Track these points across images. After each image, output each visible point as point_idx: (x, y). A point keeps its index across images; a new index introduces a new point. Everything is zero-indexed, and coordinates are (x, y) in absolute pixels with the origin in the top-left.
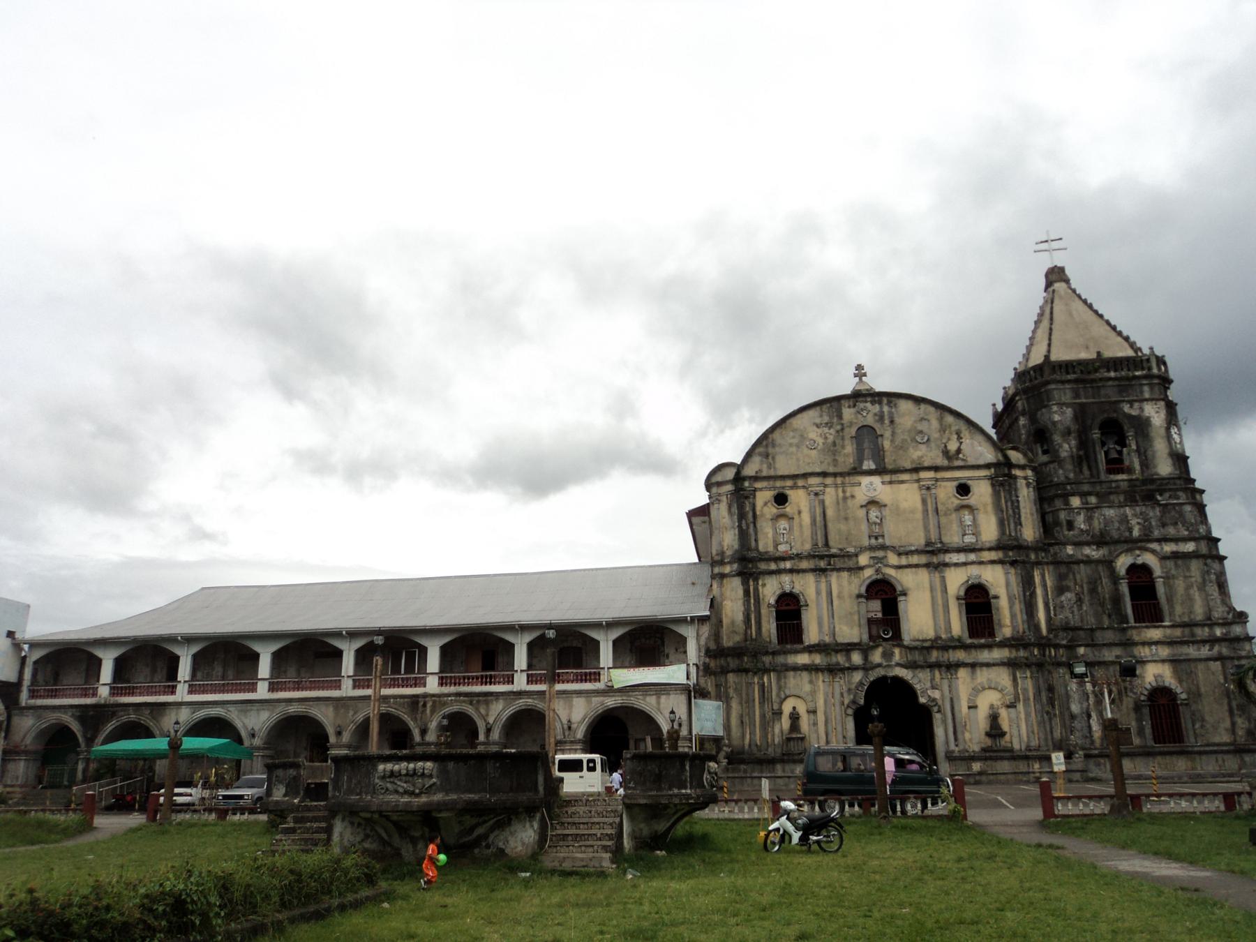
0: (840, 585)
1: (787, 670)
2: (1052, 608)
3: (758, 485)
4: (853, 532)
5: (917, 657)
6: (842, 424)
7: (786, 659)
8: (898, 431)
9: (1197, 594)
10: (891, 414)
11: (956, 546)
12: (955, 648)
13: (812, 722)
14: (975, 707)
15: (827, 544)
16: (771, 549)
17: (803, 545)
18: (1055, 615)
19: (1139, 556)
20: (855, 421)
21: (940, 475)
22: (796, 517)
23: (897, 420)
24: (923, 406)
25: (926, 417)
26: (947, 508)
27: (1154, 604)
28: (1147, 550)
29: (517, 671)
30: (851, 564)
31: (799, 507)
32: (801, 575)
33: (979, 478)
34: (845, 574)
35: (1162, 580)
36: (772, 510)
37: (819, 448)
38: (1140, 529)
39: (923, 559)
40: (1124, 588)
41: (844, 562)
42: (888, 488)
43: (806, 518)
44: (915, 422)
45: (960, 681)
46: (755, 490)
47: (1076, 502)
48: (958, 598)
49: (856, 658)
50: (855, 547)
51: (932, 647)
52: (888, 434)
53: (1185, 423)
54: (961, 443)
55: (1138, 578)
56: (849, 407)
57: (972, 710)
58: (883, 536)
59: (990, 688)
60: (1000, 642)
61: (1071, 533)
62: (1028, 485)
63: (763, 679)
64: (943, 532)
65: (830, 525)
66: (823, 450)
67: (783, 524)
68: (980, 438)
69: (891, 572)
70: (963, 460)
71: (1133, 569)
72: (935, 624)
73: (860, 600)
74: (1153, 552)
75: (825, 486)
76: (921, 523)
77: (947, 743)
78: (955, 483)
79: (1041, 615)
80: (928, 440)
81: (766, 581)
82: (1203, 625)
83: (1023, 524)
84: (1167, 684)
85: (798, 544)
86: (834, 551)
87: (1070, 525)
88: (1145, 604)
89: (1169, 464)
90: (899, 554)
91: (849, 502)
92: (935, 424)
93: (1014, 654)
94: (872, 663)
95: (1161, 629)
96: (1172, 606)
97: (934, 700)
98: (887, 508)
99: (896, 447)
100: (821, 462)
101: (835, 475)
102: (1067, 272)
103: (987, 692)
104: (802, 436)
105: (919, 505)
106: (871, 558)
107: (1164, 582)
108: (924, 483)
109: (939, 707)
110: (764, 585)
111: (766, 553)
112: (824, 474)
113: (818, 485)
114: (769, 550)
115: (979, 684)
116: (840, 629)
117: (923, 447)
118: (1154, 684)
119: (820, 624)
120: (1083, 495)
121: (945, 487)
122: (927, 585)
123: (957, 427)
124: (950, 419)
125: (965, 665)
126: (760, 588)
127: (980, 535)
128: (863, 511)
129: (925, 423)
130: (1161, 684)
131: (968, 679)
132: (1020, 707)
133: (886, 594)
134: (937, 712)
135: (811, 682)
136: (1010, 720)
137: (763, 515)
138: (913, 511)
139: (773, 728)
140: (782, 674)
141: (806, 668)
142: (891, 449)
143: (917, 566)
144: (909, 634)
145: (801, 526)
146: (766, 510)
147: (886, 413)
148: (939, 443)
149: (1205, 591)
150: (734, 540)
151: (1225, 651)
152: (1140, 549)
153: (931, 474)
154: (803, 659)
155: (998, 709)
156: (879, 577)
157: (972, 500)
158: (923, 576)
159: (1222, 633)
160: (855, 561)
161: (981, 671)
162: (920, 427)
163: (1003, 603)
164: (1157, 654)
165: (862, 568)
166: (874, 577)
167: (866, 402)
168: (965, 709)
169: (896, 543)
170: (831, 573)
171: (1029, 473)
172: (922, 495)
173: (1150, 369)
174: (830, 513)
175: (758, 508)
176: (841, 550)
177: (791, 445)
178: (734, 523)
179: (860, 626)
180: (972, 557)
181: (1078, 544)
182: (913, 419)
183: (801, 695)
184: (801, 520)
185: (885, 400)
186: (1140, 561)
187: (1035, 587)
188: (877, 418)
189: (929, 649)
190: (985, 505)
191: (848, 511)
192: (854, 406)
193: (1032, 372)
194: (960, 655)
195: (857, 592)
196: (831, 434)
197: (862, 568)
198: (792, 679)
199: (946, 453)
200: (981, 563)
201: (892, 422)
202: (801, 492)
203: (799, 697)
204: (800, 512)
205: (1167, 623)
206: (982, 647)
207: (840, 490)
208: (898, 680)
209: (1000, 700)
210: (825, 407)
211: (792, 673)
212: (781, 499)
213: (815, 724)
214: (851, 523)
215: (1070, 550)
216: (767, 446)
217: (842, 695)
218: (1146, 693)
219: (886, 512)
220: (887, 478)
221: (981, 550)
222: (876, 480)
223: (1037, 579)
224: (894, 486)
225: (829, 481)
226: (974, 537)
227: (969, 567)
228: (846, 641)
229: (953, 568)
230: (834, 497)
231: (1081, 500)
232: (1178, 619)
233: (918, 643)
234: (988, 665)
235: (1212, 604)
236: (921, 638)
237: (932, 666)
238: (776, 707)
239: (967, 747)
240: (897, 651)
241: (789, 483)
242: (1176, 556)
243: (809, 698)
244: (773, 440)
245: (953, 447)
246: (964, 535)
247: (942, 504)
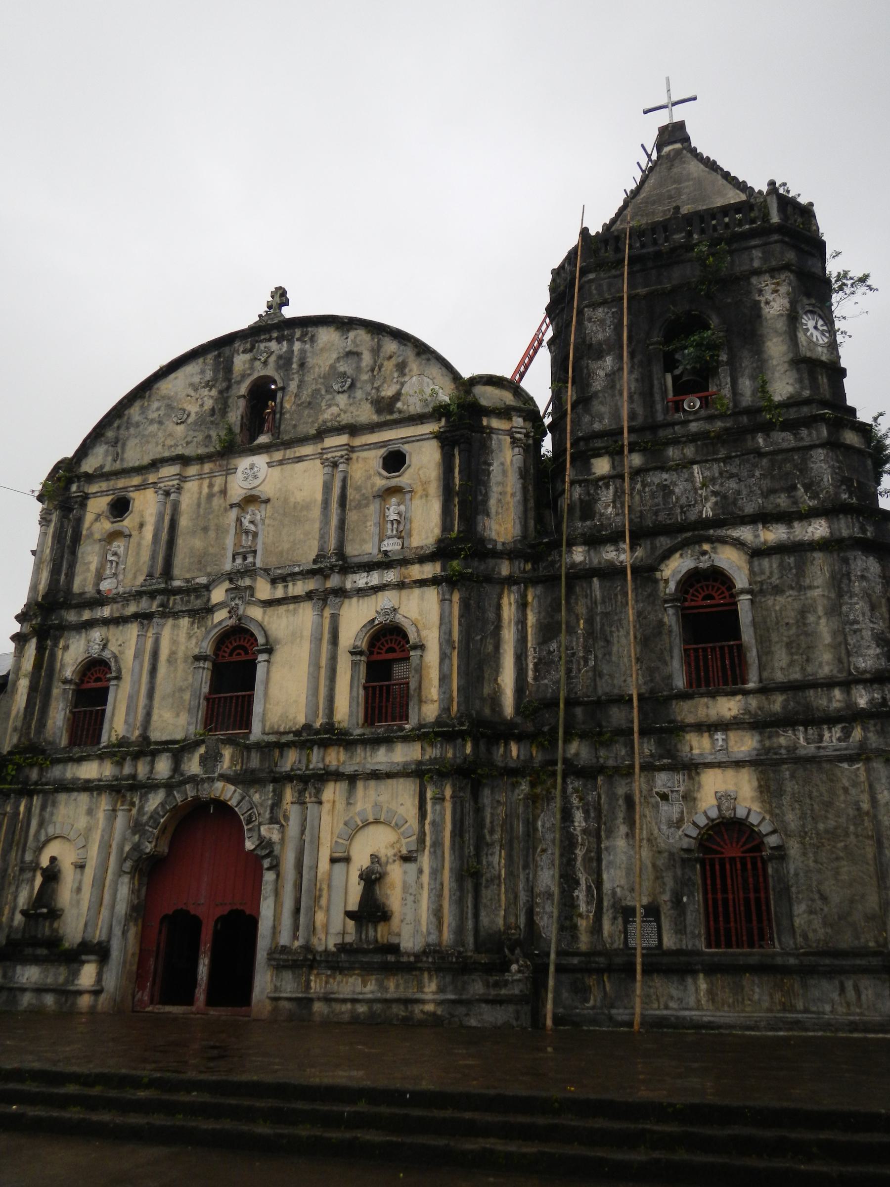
0: (174, 642)
2: (531, 666)
3: (93, 488)
4: (211, 550)
5: (255, 761)
6: (229, 380)
7: (64, 773)
8: (309, 378)
9: (823, 621)
10: (303, 352)
11: (365, 559)
12: (325, 744)
13: (76, 885)
14: (347, 860)
15: (168, 572)
16: (90, 589)
17: (135, 577)
18: (535, 679)
19: (704, 553)
20: (248, 372)
21: (358, 441)
22: (135, 533)
23: (311, 361)
24: (352, 335)
25: (355, 350)
26: (364, 495)
27: (731, 647)
28: (723, 541)
30: (198, 604)
31: (142, 516)
32: (121, 628)
33: (421, 439)
34: (185, 622)
35: (749, 597)
36: (107, 526)
37: (190, 420)
38: (716, 503)
39: (311, 585)
40: (670, 618)
41: (189, 601)
42: (276, 471)
43: (148, 533)
44: (338, 359)
45: (326, 807)
46: (86, 497)
47: (602, 466)
48: (352, 653)
49: (163, 767)
50: (209, 575)
51: (289, 745)
52: (293, 386)
54: (402, 384)
55: (706, 598)
56: (244, 352)
57: (339, 867)
58: (255, 552)
59: (377, 822)
60: (412, 730)
61: (588, 523)
62: (514, 442)
63: (18, 807)
64: (349, 536)
65: (180, 542)
66: (195, 423)
67: (119, 546)
68: (435, 370)
69: (256, 613)
70: (400, 412)
71: (692, 579)
73: (196, 664)
74: (739, 544)
75: (183, 479)
76: (317, 525)
77: (275, 930)
78: (382, 452)
79: (507, 679)
80: (352, 386)
81: (71, 641)
82: (829, 684)
83: (493, 510)
84: (741, 813)
85: (130, 576)
86: (177, 583)
87: (587, 509)
88: (713, 649)
89: (791, 381)
90: (274, 582)
91: (217, 502)
92: (367, 359)
93: (432, 752)
94: (182, 775)
95: (739, 697)
96: (765, 652)
97: (270, 844)
98: (269, 506)
99: (299, 405)
100: (188, 443)
101: (201, 459)
102: (690, 130)
103: (372, 829)
104: (169, 407)
105: (319, 496)
107: (752, 601)
108: (329, 456)
109: (277, 858)
110: (66, 648)
111: (82, 594)
112: (184, 460)
113: (170, 478)
114: (86, 590)
115: (359, 814)
116: (161, 716)
117: (342, 399)
118: (714, 814)
119: (131, 708)
120: (616, 453)
121: (365, 459)
122: (307, 633)
123: (400, 359)
124: (391, 346)
125: (336, 776)
126: (60, 653)
127: (410, 535)
128: (233, 514)
129: (352, 361)
130: (728, 814)
131: (341, 805)
132: (425, 860)
133: (247, 653)
134: (269, 869)
135: (90, 812)
136: (405, 888)
137: (90, 535)
138: (307, 507)
139: (15, 898)
140: (51, 797)
141: (88, 787)
142: (294, 407)
143: (296, 599)
144: (263, 721)
145: (139, 544)
146: (97, 526)
147: (296, 353)
148: (368, 387)
149: (840, 614)
151: (874, 741)
152: (709, 540)
153: (343, 439)
154: (90, 771)
155: (387, 862)
157: (405, 479)
158: (306, 615)
159: (871, 701)
160: (205, 600)
161: (365, 788)
162: (342, 367)
163: (432, 657)
164: (725, 749)
166: (224, 624)
167: (270, 340)
168: (324, 864)
169: (273, 561)
170: (160, 621)
171: (518, 421)
173: (766, 217)
174: (184, 522)
175: (86, 524)
176: (187, 581)
177: (152, 422)
179: (189, 711)
180: (391, 576)
181: (594, 541)
182: (335, 356)
183: (72, 836)
184: (142, 538)
185: (298, 333)
186: (704, 563)
187: (498, 627)
188: (281, 362)
189: (282, 747)
190: (425, 484)
191: (211, 517)
192: (251, 350)
194: (335, 758)
195: (196, 651)
196: (208, 398)
197: (210, 610)
198: (63, 803)
200: (401, 586)
201: (302, 365)
202: (150, 493)
203: (69, 840)
204: (141, 525)
205: (751, 685)
206: (375, 742)
207: (206, 483)
208: (221, 806)
209: (392, 846)
210: (210, 358)
211: (62, 797)
213: (79, 890)
214: (212, 534)
215: (579, 555)
216: (119, 428)
218: (694, 833)
220: (278, 455)
221: (404, 562)
222: (260, 461)
223: (509, 611)
224: (288, 467)
225: (192, 470)
226: (400, 541)
227: (380, 594)
228: (165, 738)
229: (355, 600)
230: (196, 496)
231: (613, 463)
232: (779, 677)
233: (272, 738)
234: (376, 775)
235: (852, 640)
236: (282, 730)
237: (280, 780)
238: (28, 857)
239: (315, 941)
240: (227, 753)
241: (136, 480)
242: (780, 549)
244: (129, 418)
245: (388, 391)
246: (381, 541)
247: (358, 489)
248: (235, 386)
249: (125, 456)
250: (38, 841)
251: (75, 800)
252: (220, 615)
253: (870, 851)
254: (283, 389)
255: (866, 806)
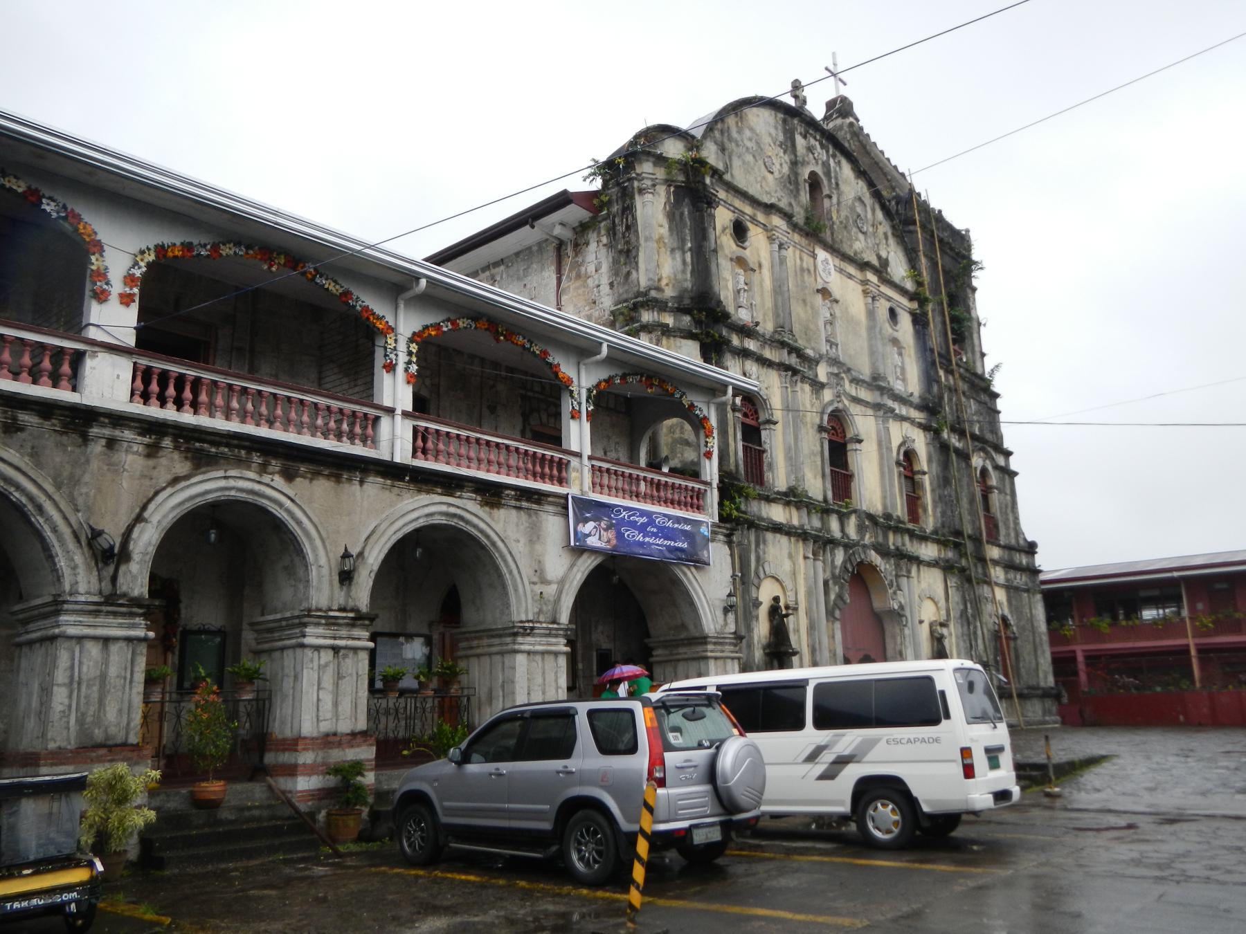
1: (767, 529)
29: (391, 411)
31: (759, 256)
48: (898, 463)
53: (985, 325)
58: (837, 345)
59: (930, 598)
72: (884, 491)
76: (865, 345)
104: (758, 143)
106: (832, 374)
133: (837, 436)
150: (684, 272)
154: (777, 513)
156: (840, 406)
165: (822, 386)
166: (836, 405)
172: (866, 304)
178: (683, 241)
179: (823, 476)
193: (893, 203)
199: (879, 257)
204: (760, 266)
211: (769, 536)
212: (740, 231)
217: (826, 583)
219: (837, 309)
220: (837, 262)
227: (904, 423)
243: (788, 583)
244: (728, 128)
248: (800, 165)
249: (733, 172)
250: (759, 578)
251: (779, 541)
252: (827, 395)
253: (1031, 638)
254: (830, 197)
255: (1029, 615)
